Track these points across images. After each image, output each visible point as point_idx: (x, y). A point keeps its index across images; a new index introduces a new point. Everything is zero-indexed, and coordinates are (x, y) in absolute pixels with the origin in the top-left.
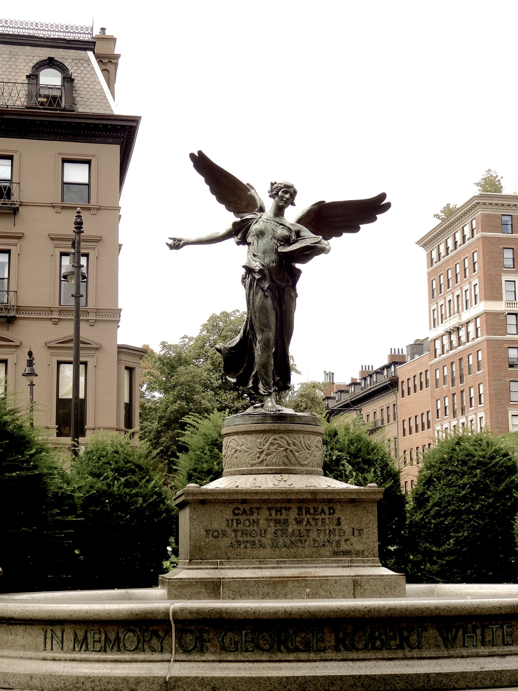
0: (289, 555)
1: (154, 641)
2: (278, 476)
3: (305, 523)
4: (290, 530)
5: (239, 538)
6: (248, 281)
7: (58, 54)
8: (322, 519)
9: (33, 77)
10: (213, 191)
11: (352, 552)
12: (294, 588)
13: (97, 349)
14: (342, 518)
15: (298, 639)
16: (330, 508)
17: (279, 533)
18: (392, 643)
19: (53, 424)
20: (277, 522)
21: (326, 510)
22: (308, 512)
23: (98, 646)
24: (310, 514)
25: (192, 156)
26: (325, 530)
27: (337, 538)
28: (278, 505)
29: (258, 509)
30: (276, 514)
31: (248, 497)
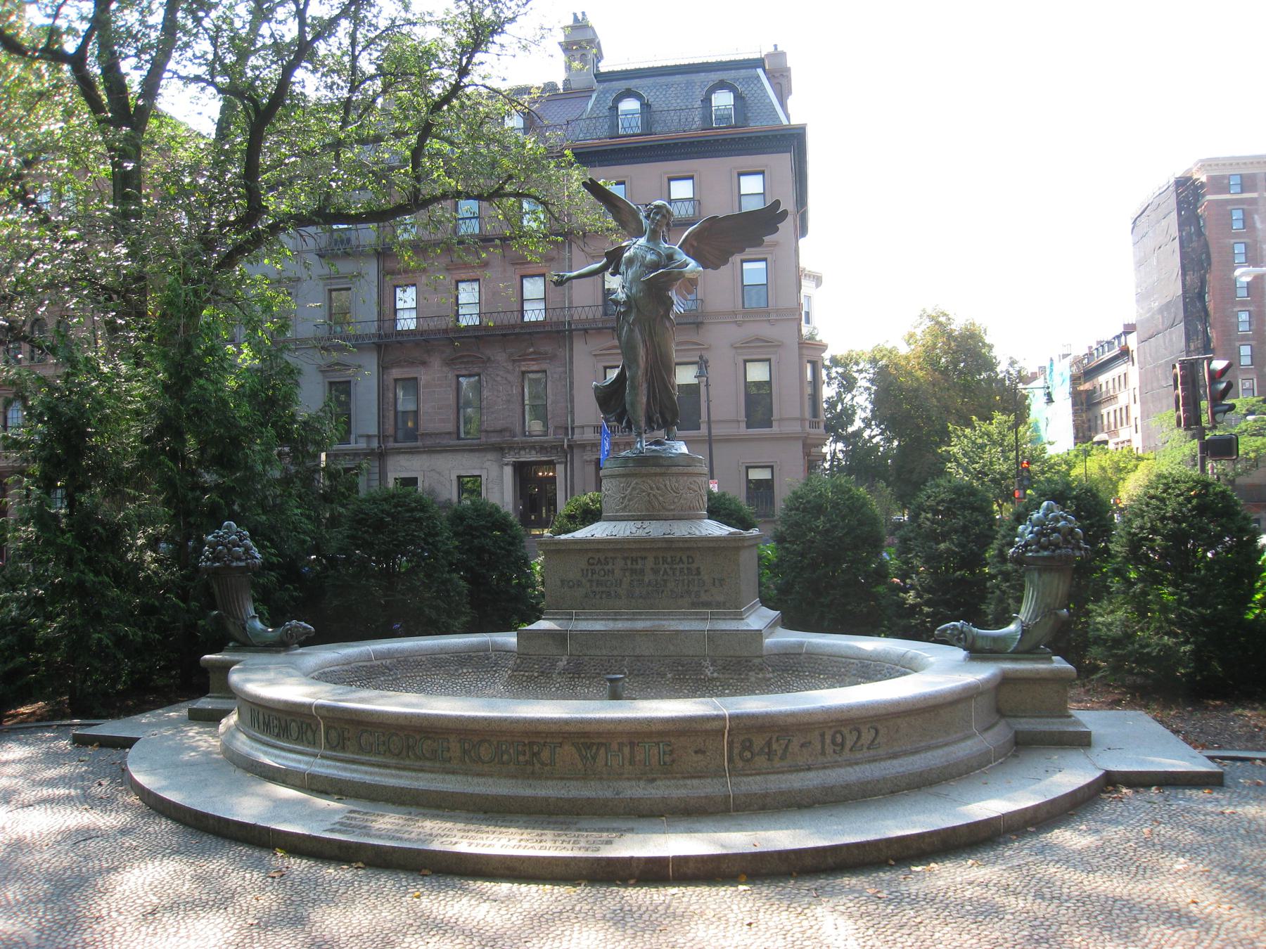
2: (639, 524)
4: (647, 580)
7: (727, 76)
9: (707, 101)
13: (778, 346)
19: (742, 417)
20: (633, 571)
21: (685, 559)
27: (696, 589)
28: (634, 555)
29: (614, 559)
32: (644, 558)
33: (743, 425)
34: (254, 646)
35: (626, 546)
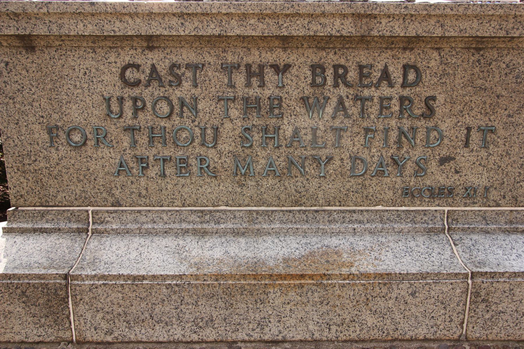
0: (283, 196)
3: (329, 110)
4: (289, 131)
5: (142, 151)
8: (381, 99)
11: (456, 191)
12: (288, 307)
14: (441, 98)
16: (406, 68)
17: (257, 137)
20: (250, 105)
21: (396, 74)
22: (340, 77)
24: (347, 85)
26: (387, 131)
27: (417, 153)
28: (254, 57)
30: (248, 85)
32: (281, 70)
35: (235, 29)
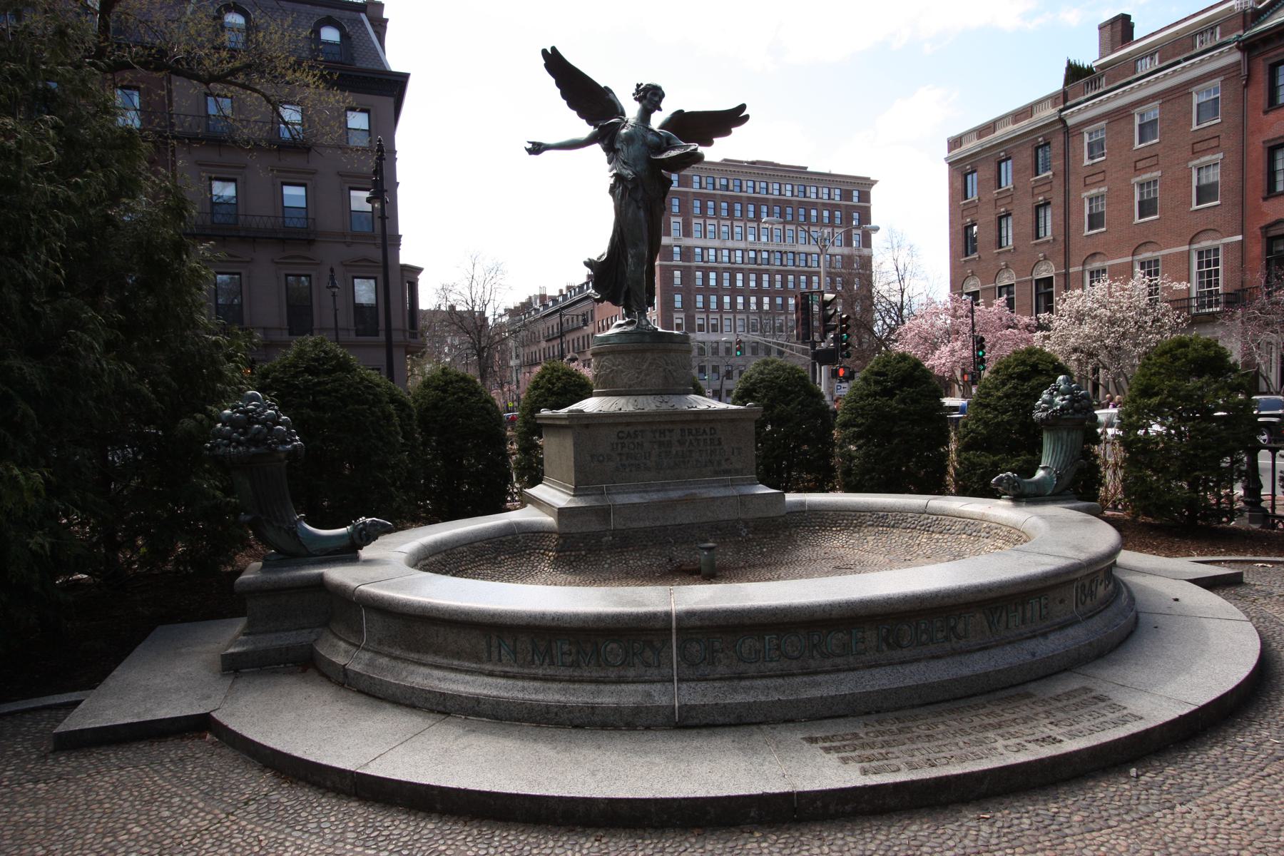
1: (648, 653)
6: (619, 191)
9: (317, 32)
10: (564, 95)
15: (834, 641)
18: (940, 635)
20: (661, 444)
22: (690, 433)
23: (569, 659)
25: (544, 52)
31: (633, 420)
33: (353, 334)
34: (310, 555)
